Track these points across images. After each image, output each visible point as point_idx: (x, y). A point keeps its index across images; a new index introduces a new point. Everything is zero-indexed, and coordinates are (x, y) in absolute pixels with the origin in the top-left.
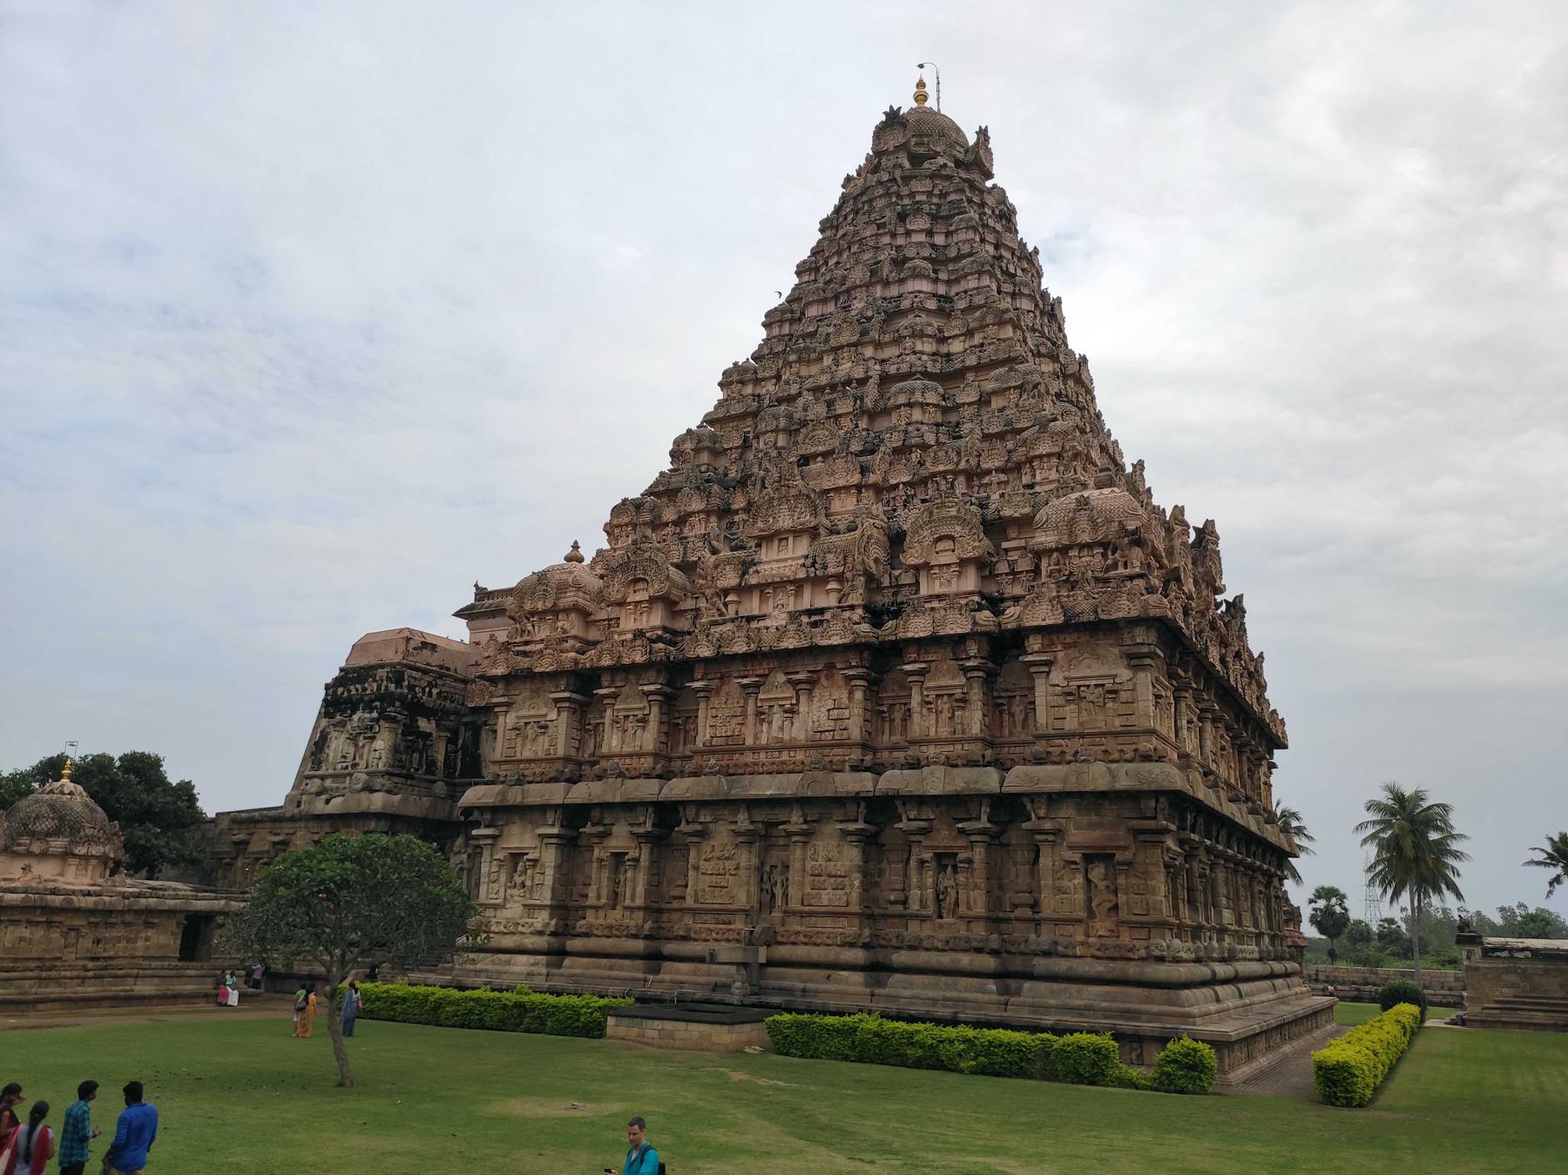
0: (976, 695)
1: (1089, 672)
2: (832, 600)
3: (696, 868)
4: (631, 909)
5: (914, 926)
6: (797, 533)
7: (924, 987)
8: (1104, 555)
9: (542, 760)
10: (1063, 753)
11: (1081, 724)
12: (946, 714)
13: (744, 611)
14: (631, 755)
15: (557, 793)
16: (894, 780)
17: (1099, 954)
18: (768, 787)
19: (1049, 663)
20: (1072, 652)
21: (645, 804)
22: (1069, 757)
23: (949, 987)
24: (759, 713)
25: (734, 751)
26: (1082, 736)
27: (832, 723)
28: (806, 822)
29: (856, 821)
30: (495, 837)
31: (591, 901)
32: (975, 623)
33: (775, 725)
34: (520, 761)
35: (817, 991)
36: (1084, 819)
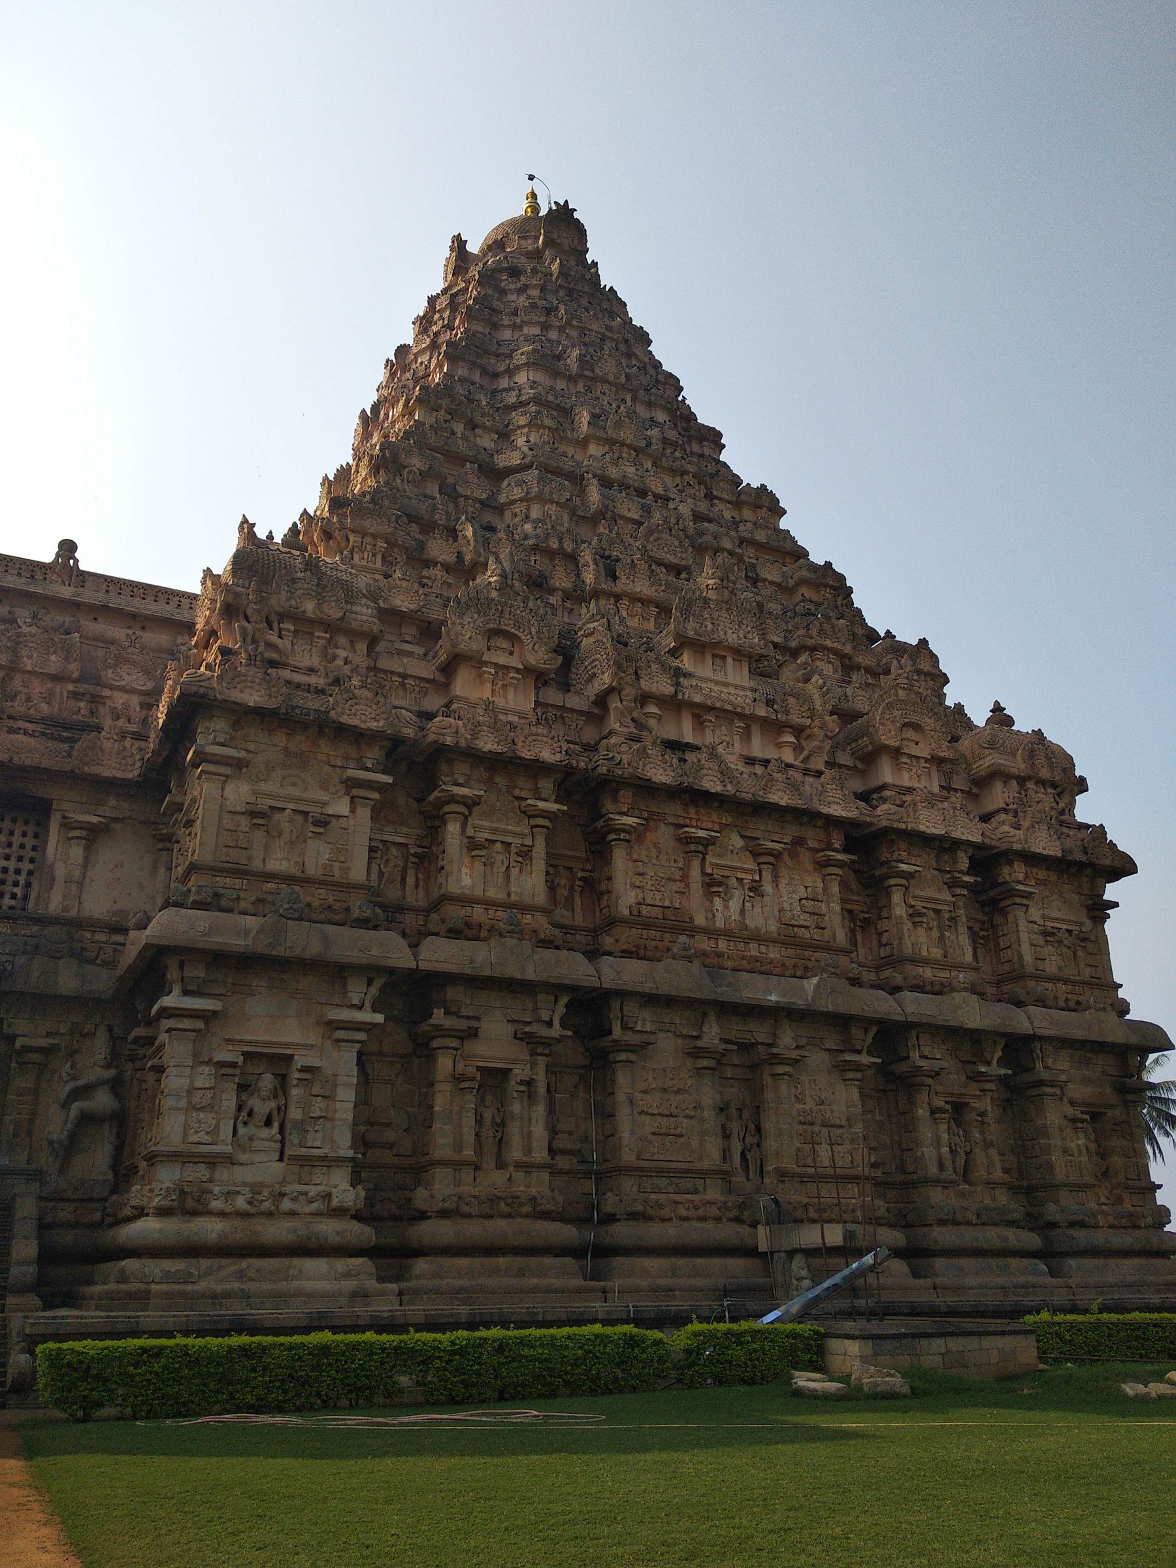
4: (527, 1167)
5: (936, 1195)
6: (739, 653)
9: (322, 883)
10: (1055, 997)
11: (1059, 968)
12: (935, 934)
13: (671, 734)
14: (507, 906)
15: (389, 948)
16: (914, 1006)
19: (1028, 896)
21: (556, 989)
22: (1061, 1003)
24: (712, 885)
25: (681, 931)
28: (797, 1047)
29: (859, 1052)
30: (208, 1017)
33: (735, 905)
34: (271, 876)
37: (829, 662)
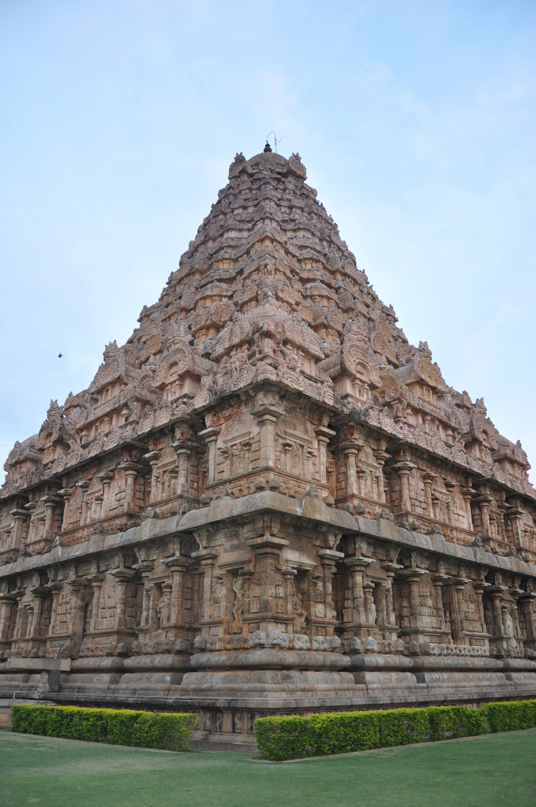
0: (183, 466)
1: (237, 434)
2: (122, 421)
3: (56, 611)
7: (137, 681)
8: (249, 349)
17: (228, 646)
18: (77, 551)
20: (230, 422)
23: (148, 679)
26: (230, 481)
27: (116, 503)
29: (118, 567)
31: (15, 638)
32: (173, 415)
35: (84, 688)
36: (228, 545)
37: (202, 335)
